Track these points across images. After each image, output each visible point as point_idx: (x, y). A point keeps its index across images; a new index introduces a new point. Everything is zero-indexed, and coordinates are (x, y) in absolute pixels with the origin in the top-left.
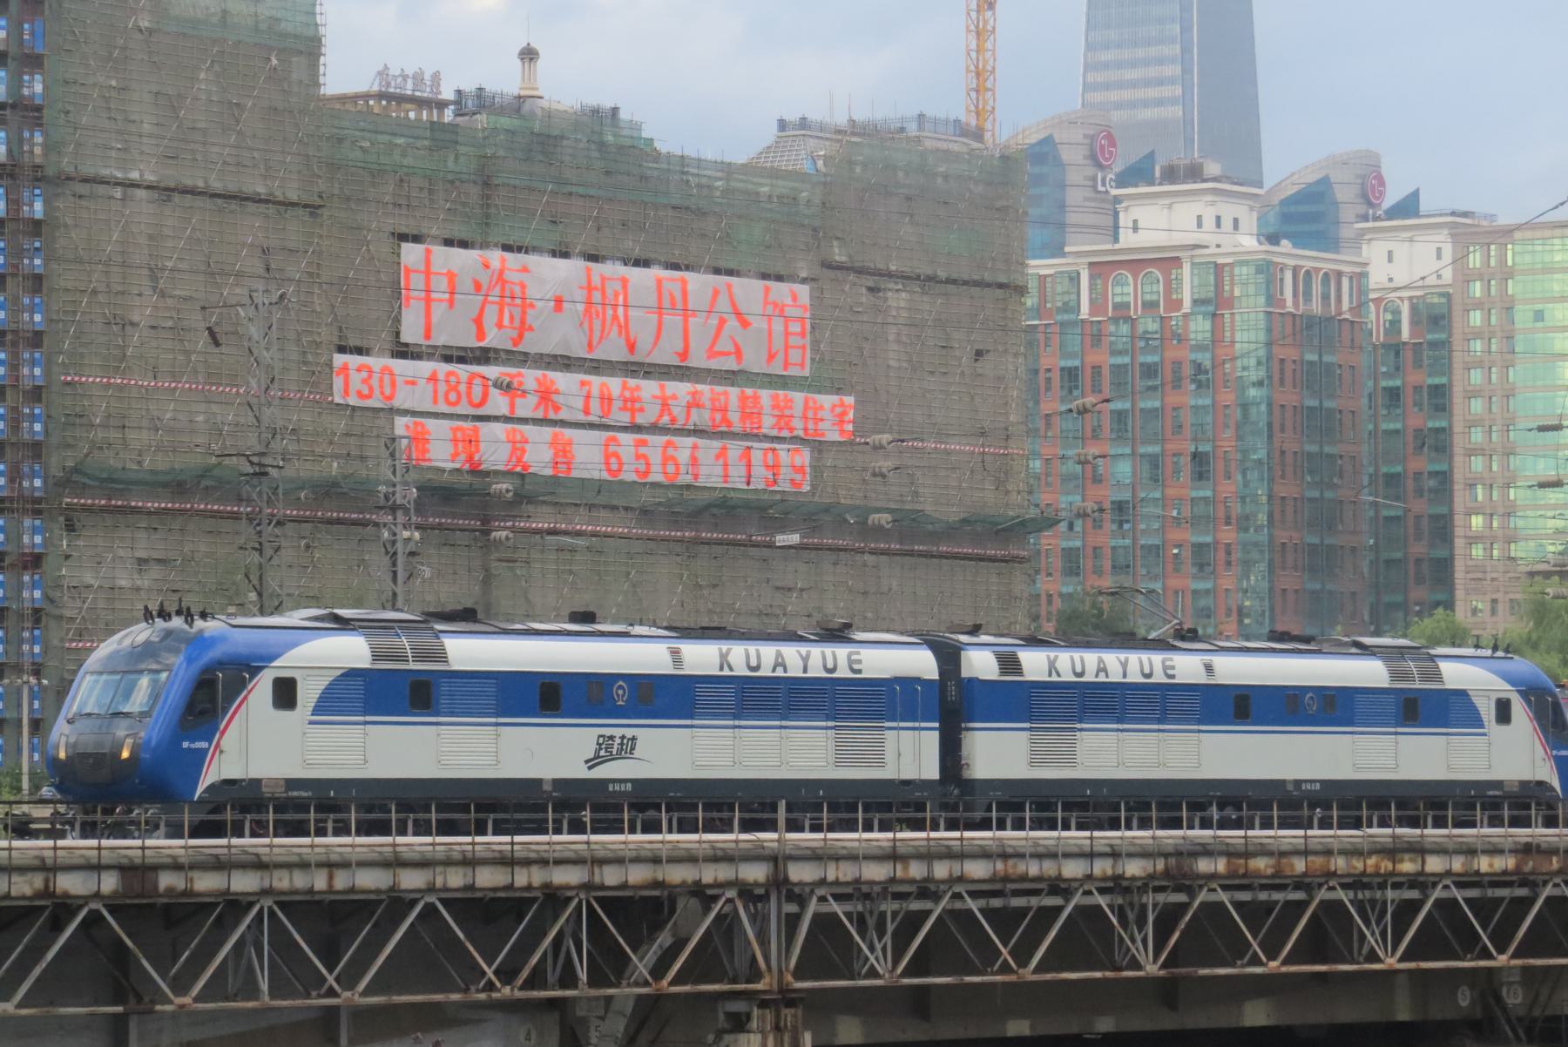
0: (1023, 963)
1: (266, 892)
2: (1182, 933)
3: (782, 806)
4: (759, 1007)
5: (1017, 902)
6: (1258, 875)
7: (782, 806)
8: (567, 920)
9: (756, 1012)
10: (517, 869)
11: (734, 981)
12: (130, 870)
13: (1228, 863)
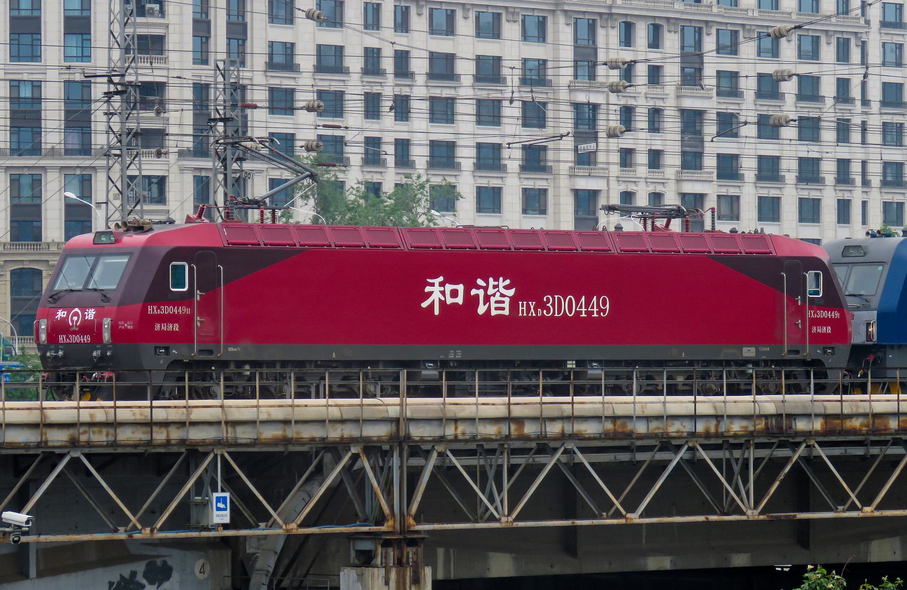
0: (631, 509)
2: (782, 482)
3: (403, 374)
4: (383, 546)
5: (640, 456)
6: (854, 432)
7: (403, 374)
8: (206, 470)
10: (155, 429)
11: (366, 521)
13: (826, 423)
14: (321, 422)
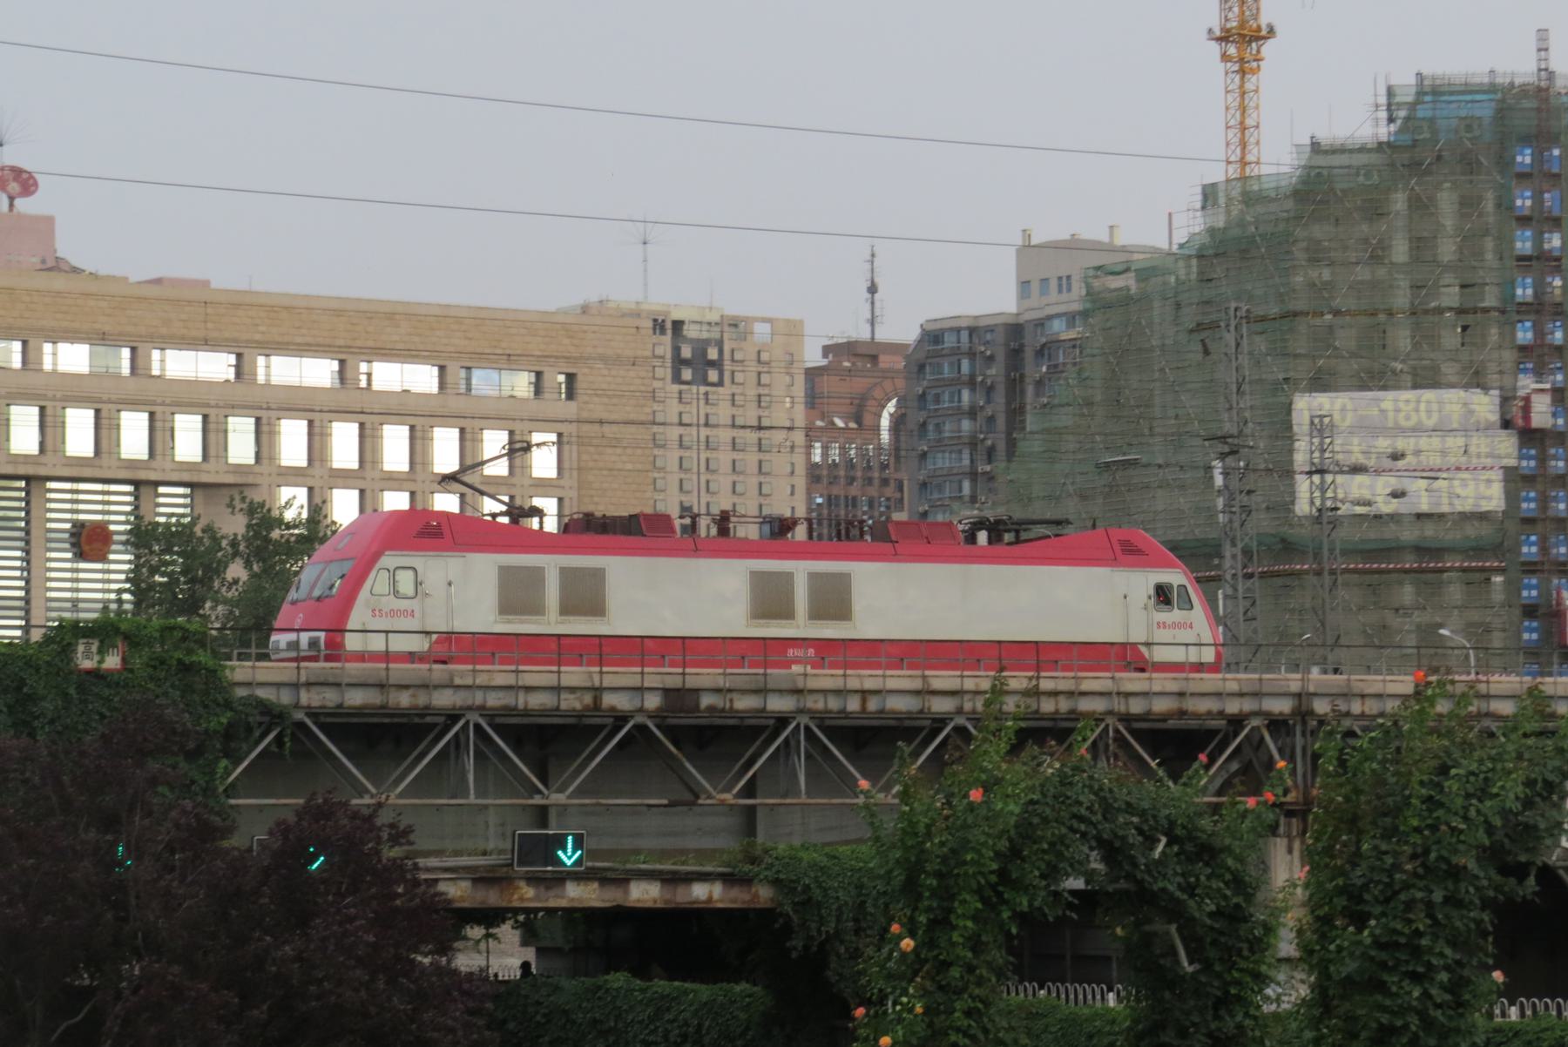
1: (801, 711)
9: (1282, 820)
12: (666, 692)
14: (1218, 695)
